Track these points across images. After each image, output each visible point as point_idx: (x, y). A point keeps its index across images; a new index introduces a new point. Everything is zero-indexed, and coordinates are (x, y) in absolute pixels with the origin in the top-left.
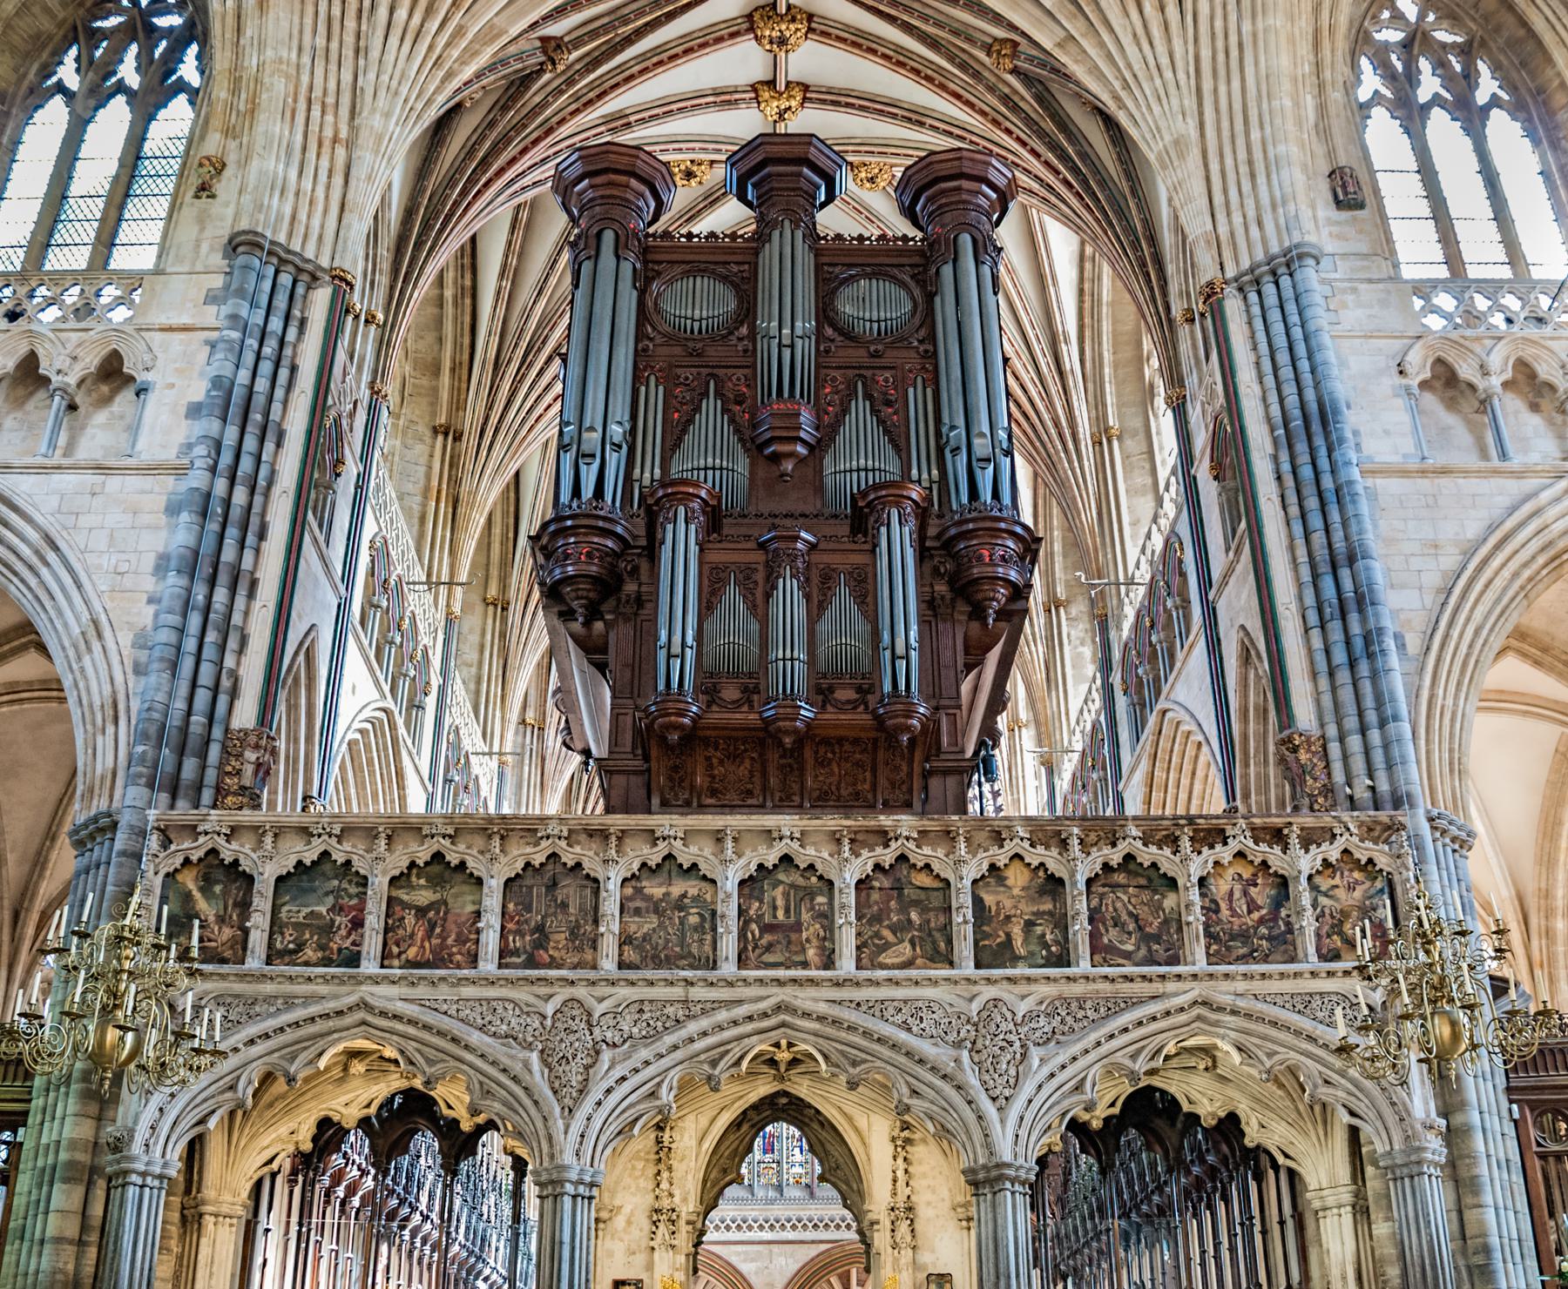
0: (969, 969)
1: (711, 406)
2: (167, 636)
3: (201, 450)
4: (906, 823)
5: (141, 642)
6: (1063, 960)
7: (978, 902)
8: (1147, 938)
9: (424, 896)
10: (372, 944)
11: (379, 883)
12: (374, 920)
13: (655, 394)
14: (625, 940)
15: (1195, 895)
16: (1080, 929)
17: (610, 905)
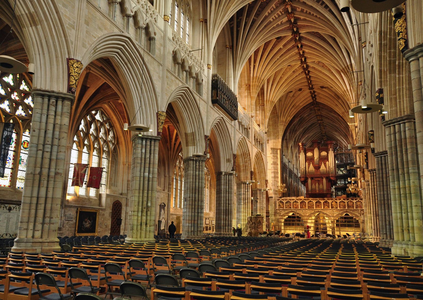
0: (330, 208)
1: (311, 164)
2: (274, 183)
3: (273, 168)
4: (326, 199)
5: (272, 184)
6: (337, 208)
7: (331, 204)
8: (343, 206)
9: (295, 203)
10: (292, 207)
11: (292, 203)
12: (292, 206)
13: (307, 163)
14: (308, 206)
15: (346, 204)
16: (338, 206)
17: (307, 204)
